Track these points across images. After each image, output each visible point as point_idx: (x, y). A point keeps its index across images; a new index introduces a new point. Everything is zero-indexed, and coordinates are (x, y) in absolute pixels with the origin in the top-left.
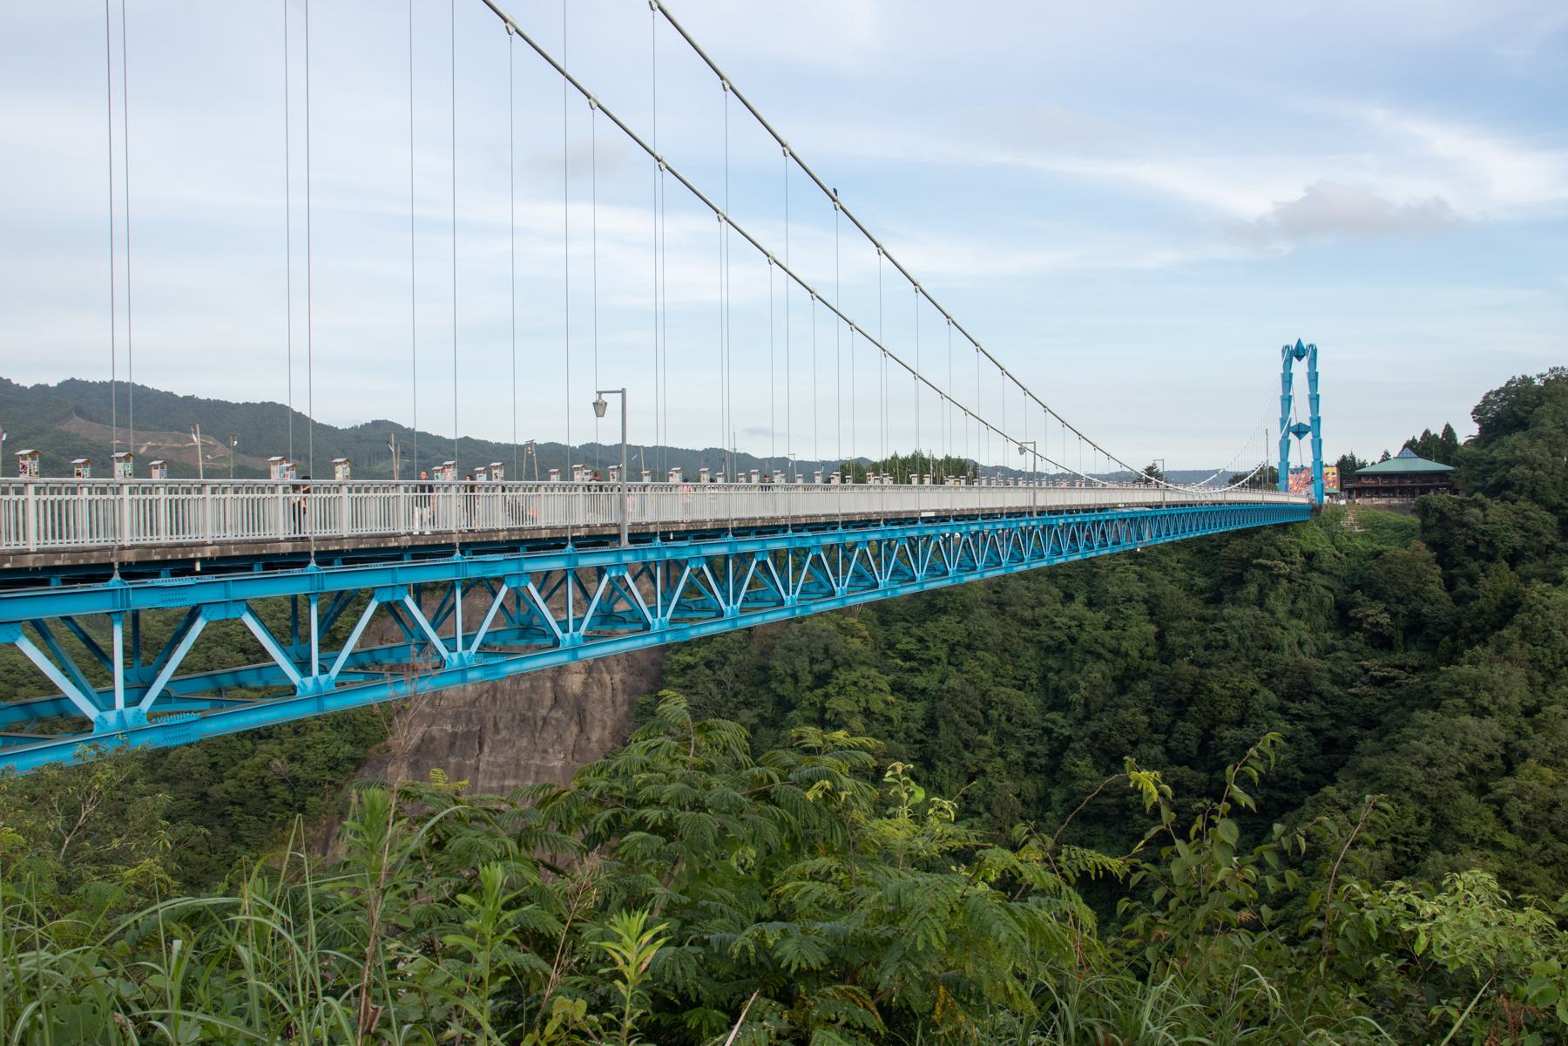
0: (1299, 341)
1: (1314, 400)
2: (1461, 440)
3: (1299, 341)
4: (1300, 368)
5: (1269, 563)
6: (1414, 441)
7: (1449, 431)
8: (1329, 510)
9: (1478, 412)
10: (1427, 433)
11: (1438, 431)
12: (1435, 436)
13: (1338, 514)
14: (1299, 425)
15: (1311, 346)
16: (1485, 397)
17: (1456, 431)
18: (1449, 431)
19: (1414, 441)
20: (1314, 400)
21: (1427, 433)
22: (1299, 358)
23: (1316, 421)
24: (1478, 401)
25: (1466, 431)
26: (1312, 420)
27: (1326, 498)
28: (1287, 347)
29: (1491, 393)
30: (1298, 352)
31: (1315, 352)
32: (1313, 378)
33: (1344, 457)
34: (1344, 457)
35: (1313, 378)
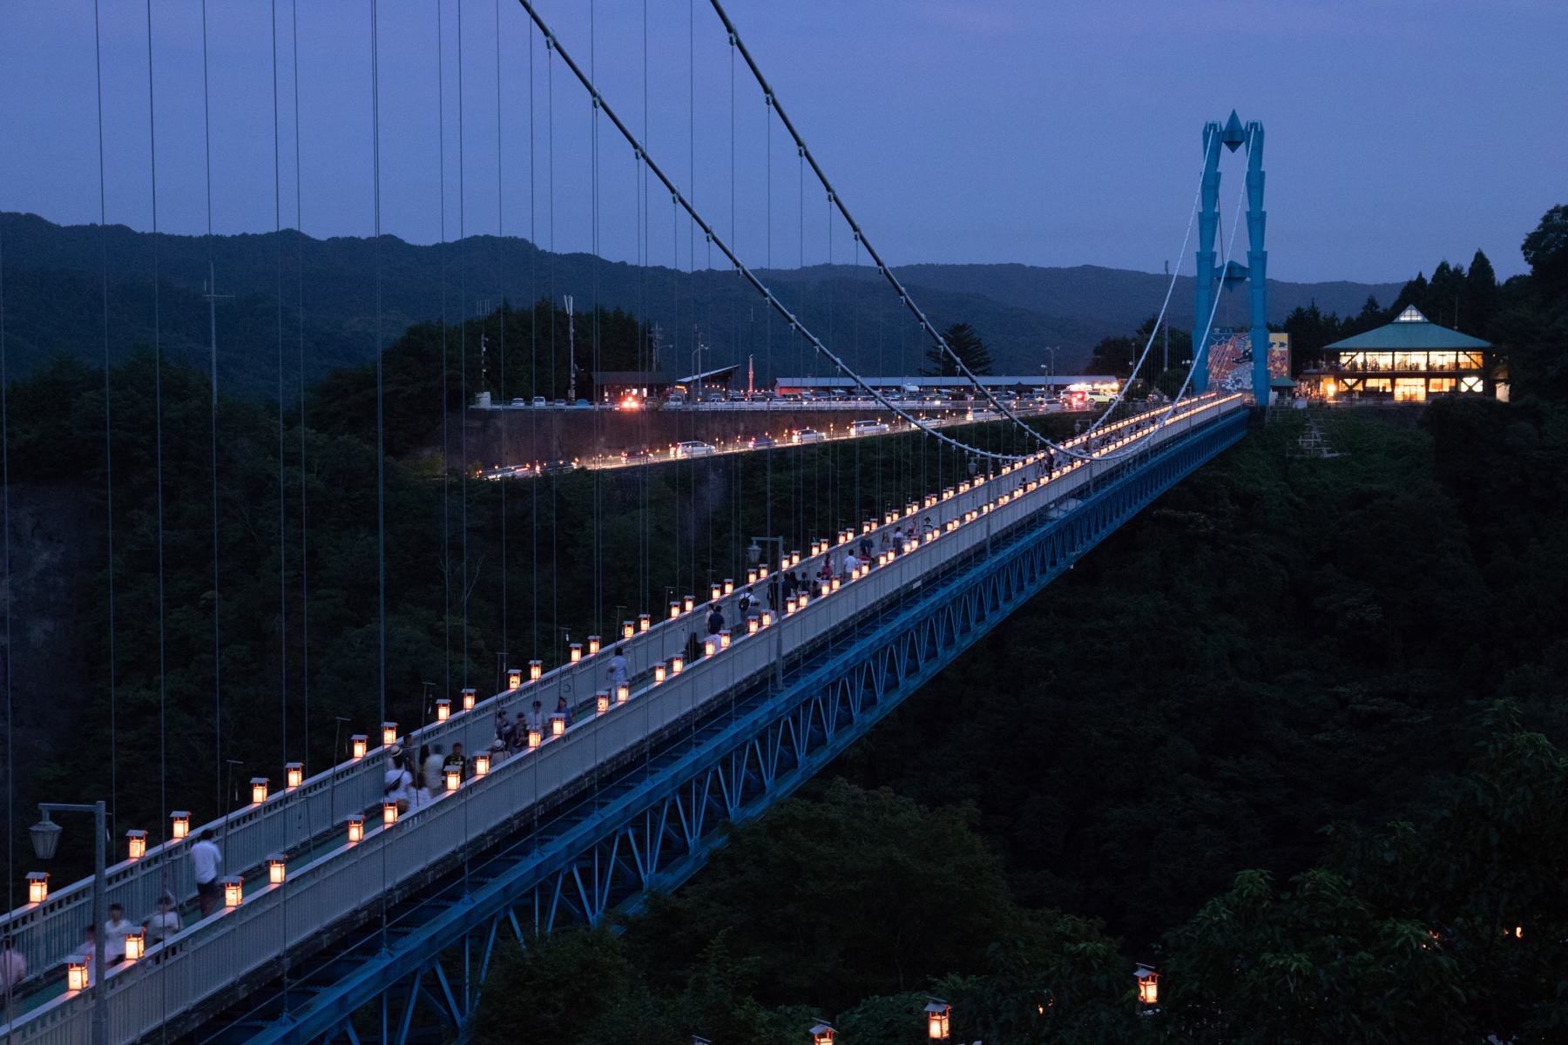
0: (1234, 117)
1: (1256, 221)
2: (1501, 277)
3: (1234, 117)
4: (1234, 163)
5: (1180, 514)
6: (1421, 280)
7: (1481, 263)
8: (1278, 418)
9: (1533, 246)
10: (1443, 267)
11: (1465, 262)
12: (1458, 272)
13: (1295, 423)
14: (1232, 266)
15: (1254, 125)
16: (1547, 219)
17: (1493, 264)
18: (1481, 263)
19: (1421, 280)
20: (1256, 221)
21: (1443, 267)
22: (1233, 145)
23: (1259, 257)
24: (1533, 225)
25: (1510, 265)
26: (1251, 256)
27: (1273, 395)
28: (1213, 126)
29: (1556, 210)
30: (1231, 135)
31: (1260, 135)
32: (1256, 183)
33: (1299, 310)
34: (1299, 310)
35: (1256, 183)
